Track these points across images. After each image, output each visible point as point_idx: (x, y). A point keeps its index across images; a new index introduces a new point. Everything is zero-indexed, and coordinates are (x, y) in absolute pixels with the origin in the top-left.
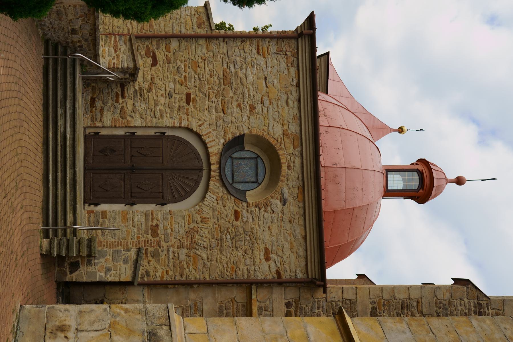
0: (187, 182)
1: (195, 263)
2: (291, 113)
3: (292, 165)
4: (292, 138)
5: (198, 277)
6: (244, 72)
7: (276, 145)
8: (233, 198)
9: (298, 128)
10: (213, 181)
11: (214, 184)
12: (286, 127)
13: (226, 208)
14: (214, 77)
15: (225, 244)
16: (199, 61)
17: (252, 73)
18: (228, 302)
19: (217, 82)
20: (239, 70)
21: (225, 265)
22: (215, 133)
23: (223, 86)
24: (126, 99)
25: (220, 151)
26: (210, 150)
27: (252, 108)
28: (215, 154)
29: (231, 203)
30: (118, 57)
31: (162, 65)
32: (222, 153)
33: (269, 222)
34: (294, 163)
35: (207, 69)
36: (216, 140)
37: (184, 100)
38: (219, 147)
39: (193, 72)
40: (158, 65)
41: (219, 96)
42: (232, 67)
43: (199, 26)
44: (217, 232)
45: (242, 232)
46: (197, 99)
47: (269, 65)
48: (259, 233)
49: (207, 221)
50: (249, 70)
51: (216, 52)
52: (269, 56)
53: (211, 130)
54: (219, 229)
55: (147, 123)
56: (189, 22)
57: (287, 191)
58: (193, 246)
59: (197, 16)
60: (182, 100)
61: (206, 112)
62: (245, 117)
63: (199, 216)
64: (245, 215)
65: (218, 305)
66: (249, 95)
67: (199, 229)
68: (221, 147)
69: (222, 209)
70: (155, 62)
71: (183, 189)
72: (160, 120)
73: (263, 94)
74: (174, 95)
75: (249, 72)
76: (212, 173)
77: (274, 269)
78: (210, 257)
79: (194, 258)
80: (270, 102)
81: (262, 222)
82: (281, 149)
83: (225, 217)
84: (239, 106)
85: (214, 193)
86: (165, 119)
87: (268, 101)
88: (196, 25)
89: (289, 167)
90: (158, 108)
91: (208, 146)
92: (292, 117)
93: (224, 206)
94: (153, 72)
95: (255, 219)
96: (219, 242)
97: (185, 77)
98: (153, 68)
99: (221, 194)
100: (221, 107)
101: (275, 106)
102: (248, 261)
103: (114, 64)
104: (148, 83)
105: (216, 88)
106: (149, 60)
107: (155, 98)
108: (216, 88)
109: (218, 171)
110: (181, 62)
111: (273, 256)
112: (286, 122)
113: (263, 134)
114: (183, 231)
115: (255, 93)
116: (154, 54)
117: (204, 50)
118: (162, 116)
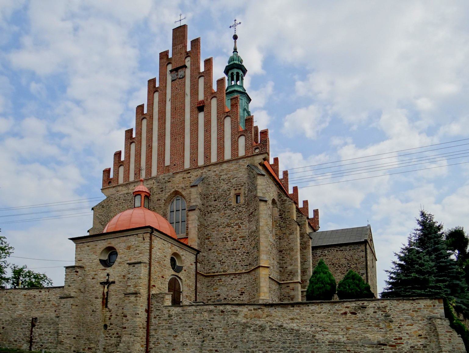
27: (165, 256)
75: (157, 254)
84: (164, 260)
89: (177, 250)
97: (158, 276)
106: (154, 288)
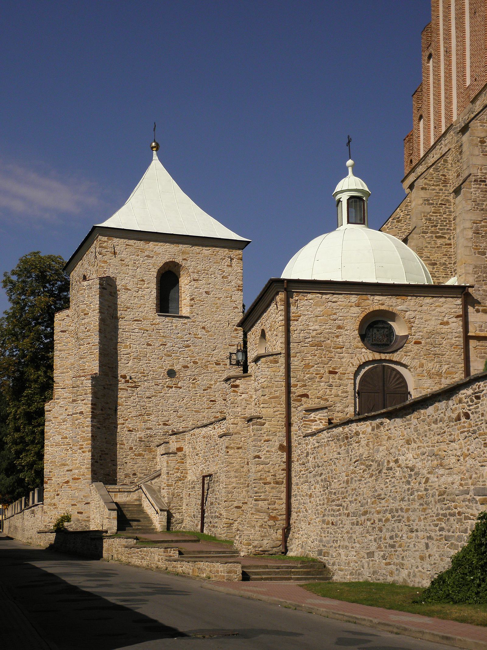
0: (393, 376)
1: (451, 373)
2: (343, 300)
3: (381, 302)
4: (361, 301)
5: (461, 372)
6: (311, 331)
7: (366, 312)
8: (405, 345)
9: (354, 296)
10: (393, 358)
11: (395, 357)
12: (353, 304)
13: (413, 350)
14: (316, 353)
15: (437, 352)
16: (305, 363)
17: (313, 326)
18: (476, 352)
19: (320, 351)
20: (310, 335)
21: (453, 352)
22: (358, 355)
23: (323, 347)
24: (334, 417)
25: (372, 352)
26: (371, 359)
27: (339, 327)
28: (374, 355)
29: (409, 346)
30: (320, 419)
31: (308, 391)
32: (373, 351)
33: (422, 321)
34: (379, 301)
35: (310, 358)
36: (363, 354)
37: (334, 375)
38: (368, 352)
39: (313, 368)
40: (307, 393)
41: (331, 350)
42: (307, 340)
43: (277, 362)
44: (430, 357)
45: (429, 340)
46: (333, 366)
47: (306, 313)
48: (430, 328)
49: (422, 364)
50: (310, 328)
51: (297, 350)
52: (299, 312)
53: (356, 358)
54: (428, 356)
55: (352, 403)
56: (274, 369)
57: (400, 307)
58: (439, 374)
59: (269, 363)
60: (334, 377)
61: (343, 360)
62: (346, 332)
63: (419, 369)
64: (417, 337)
65: (478, 359)
66: (330, 329)
67: (428, 370)
68: (368, 351)
69: (414, 352)
70: (306, 396)
71: (398, 379)
72: (349, 393)
73: (328, 319)
74: (330, 383)
75: (312, 328)
76: (387, 358)
77: (454, 319)
78: (447, 363)
79: (448, 374)
80: (335, 314)
81: (422, 326)
82: (369, 309)
83: (419, 351)
84: (337, 337)
85: (402, 358)
86: (348, 390)
87: (334, 316)
88: (276, 365)
89: (383, 304)
90: (340, 395)
91: (367, 360)
92: (345, 300)
93: (411, 351)
94: (313, 397)
95: (420, 330)
96: (436, 356)
97: (317, 374)
98: (310, 397)
99: (403, 353)
100: (339, 350)
101: (338, 311)
102: (449, 337)
103: (325, 422)
104: (322, 402)
105: (324, 352)
107: (333, 396)
108: (324, 352)
109: (386, 354)
110: (305, 376)
111: (445, 319)
112: (350, 304)
113: (359, 321)
114: (430, 381)
115: (327, 325)
116: (299, 396)
117: (296, 359)
118: (347, 392)
